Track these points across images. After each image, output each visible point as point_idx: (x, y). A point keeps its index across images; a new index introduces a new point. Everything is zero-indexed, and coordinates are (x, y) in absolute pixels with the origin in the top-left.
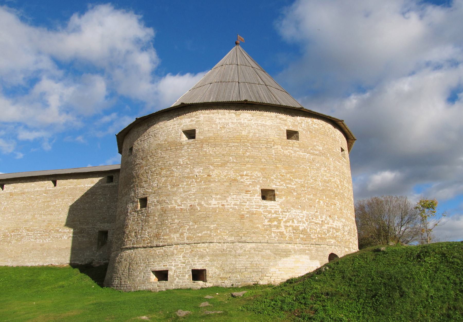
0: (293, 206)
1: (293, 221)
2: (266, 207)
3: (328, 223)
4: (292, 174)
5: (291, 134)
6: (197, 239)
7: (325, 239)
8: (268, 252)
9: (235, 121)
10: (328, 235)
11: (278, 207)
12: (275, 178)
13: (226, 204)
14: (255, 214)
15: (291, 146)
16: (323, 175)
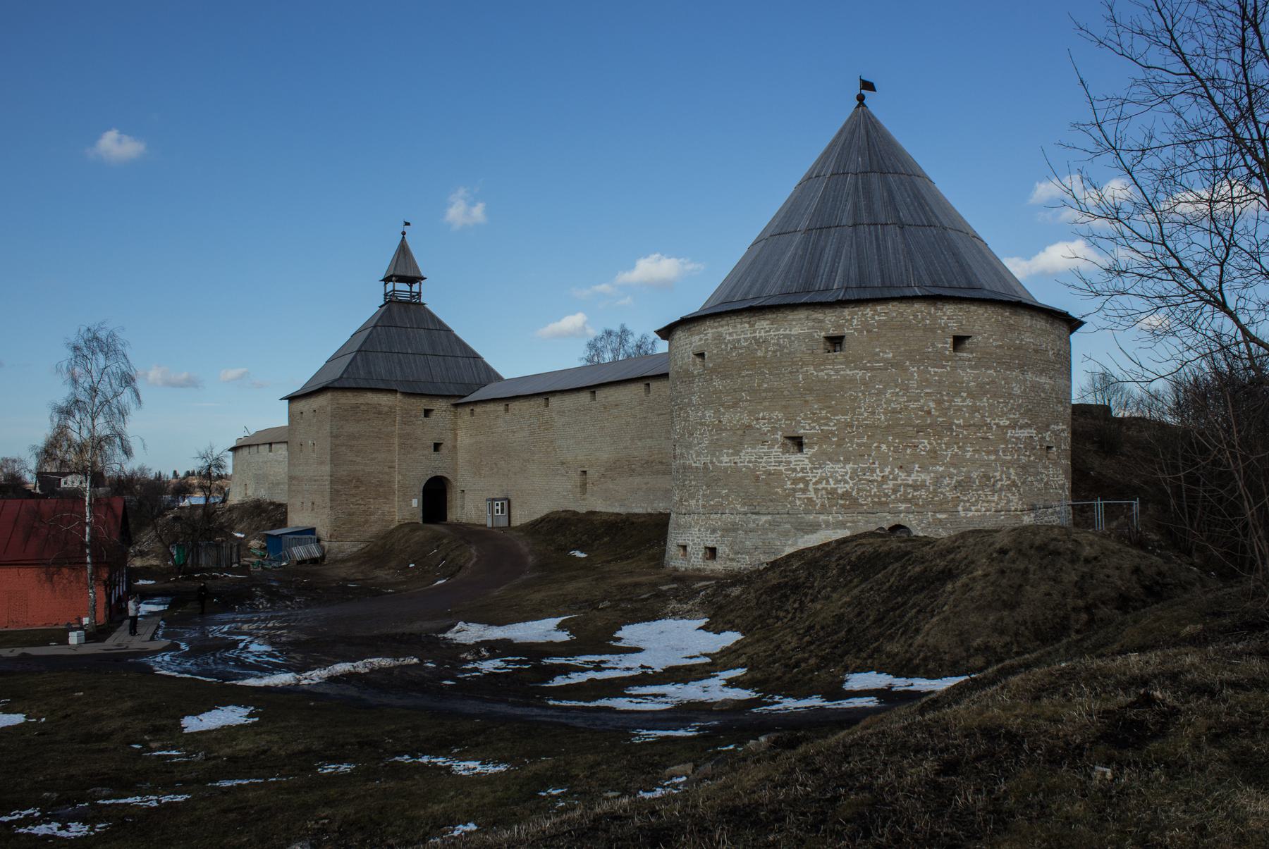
0: (830, 460)
1: (828, 482)
2: (790, 462)
3: (895, 479)
4: (830, 409)
5: (835, 342)
6: (710, 508)
7: (887, 503)
8: (788, 526)
9: (749, 335)
10: (893, 497)
11: (807, 461)
12: (803, 419)
13: (738, 461)
14: (773, 474)
15: (830, 364)
16: (889, 402)
